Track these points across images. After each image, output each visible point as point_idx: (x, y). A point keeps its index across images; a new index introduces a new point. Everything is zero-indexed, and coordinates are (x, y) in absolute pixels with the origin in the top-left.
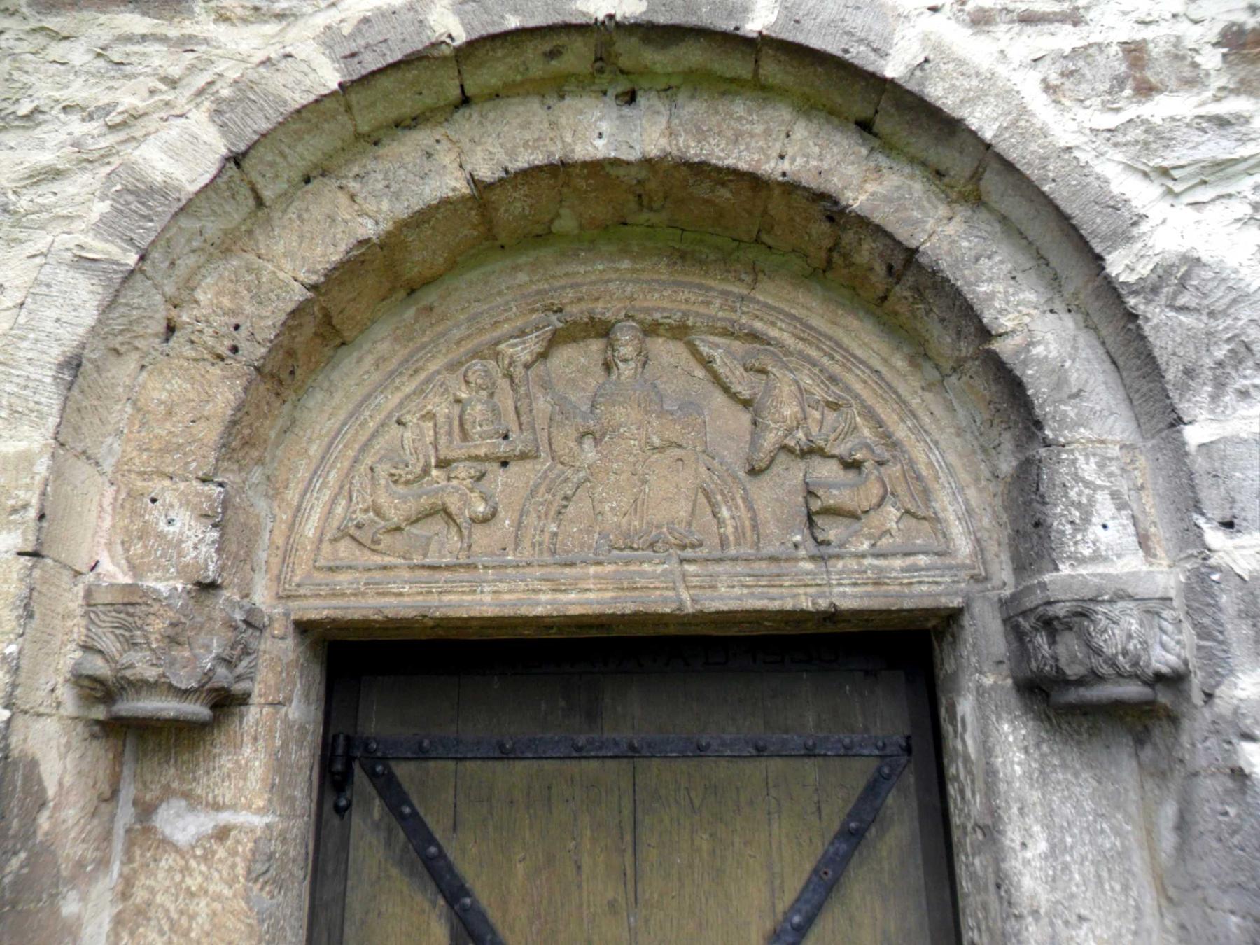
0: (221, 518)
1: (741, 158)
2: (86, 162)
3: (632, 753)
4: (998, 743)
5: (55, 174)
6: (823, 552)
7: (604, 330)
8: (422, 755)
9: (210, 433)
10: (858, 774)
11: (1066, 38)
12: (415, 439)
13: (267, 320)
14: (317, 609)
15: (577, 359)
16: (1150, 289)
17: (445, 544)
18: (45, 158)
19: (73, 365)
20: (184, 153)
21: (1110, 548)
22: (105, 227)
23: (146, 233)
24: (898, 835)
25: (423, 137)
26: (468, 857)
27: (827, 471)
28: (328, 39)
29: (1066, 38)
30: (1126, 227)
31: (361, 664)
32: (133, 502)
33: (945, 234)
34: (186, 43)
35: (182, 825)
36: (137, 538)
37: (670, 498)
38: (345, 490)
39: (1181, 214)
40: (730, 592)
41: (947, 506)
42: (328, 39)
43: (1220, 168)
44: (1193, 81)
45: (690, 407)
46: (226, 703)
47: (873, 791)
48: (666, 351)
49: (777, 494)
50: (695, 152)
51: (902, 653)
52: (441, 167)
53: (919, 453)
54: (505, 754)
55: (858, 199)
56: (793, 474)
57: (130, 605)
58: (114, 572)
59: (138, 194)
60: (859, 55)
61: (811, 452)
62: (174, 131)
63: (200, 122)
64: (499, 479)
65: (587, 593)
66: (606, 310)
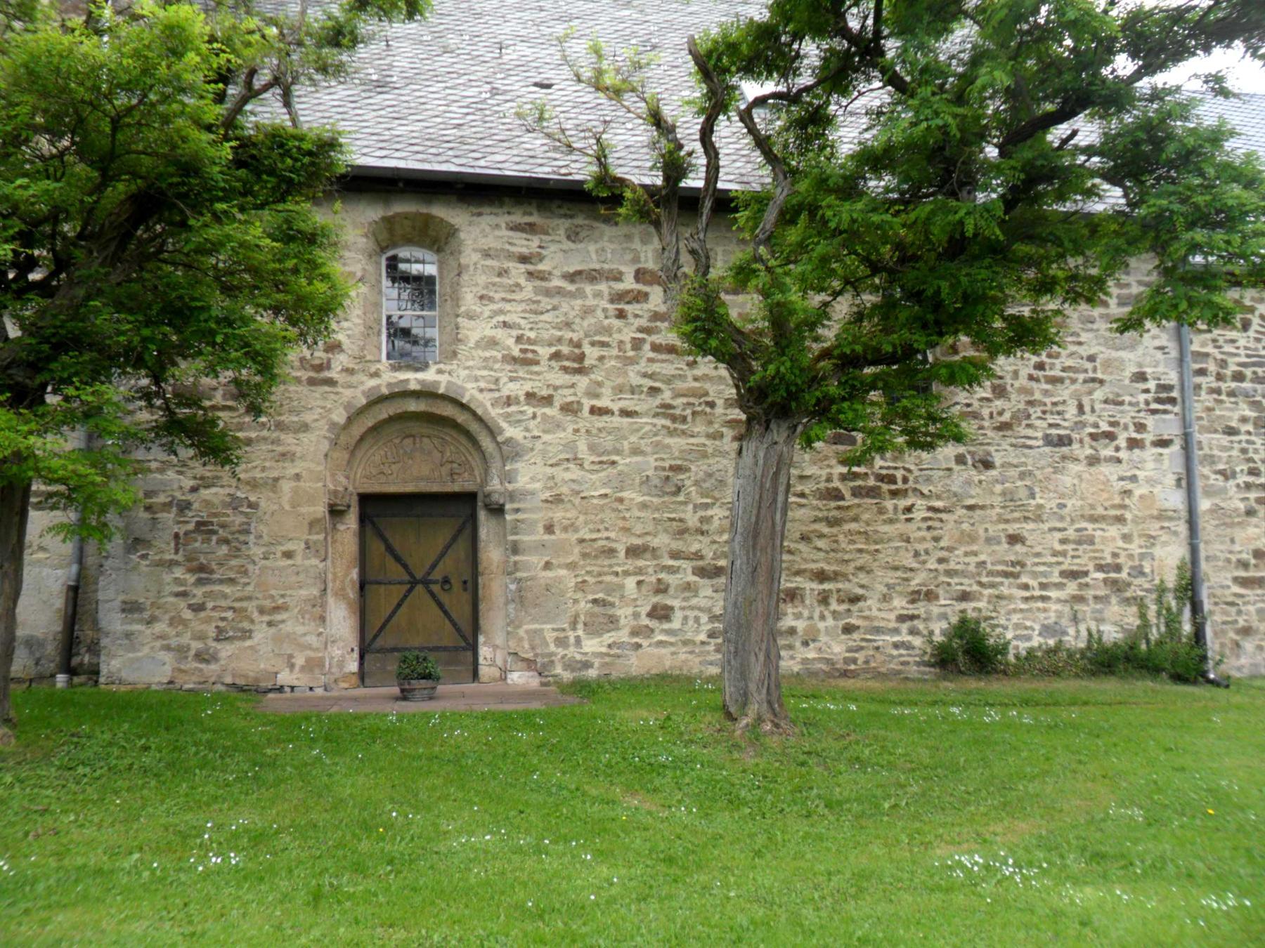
0: (347, 478)
1: (438, 412)
2: (323, 418)
3: (418, 516)
4: (482, 515)
5: (317, 420)
6: (453, 481)
7: (413, 436)
8: (378, 516)
9: (345, 463)
10: (461, 521)
11: (497, 395)
12: (377, 458)
13: (353, 442)
14: (361, 491)
15: (408, 441)
16: (504, 443)
17: (383, 479)
18: (316, 417)
19: (326, 455)
20: (340, 417)
21: (495, 484)
22: (329, 430)
23: (336, 431)
24: (468, 531)
25: (379, 406)
26: (388, 535)
27: (455, 465)
28: (363, 393)
29: (497, 395)
30: (501, 431)
31: (367, 500)
32: (333, 475)
33: (474, 427)
34: (337, 393)
35: (341, 527)
36: (334, 481)
37: (425, 470)
38: (364, 469)
39: (512, 429)
40: (436, 488)
41: (476, 473)
42: (363, 393)
43: (519, 421)
44: (518, 403)
45: (430, 453)
46: (349, 506)
47: (464, 523)
48: (426, 440)
49: (445, 470)
50: (430, 410)
51: (469, 498)
52: (384, 412)
53: (473, 464)
54: (394, 515)
55: (459, 421)
56: (449, 466)
57: (335, 492)
58: (332, 487)
59: (333, 425)
60: (459, 398)
61: (452, 462)
62: (337, 412)
63: (341, 410)
64: (393, 467)
65: (410, 488)
66: (413, 432)
